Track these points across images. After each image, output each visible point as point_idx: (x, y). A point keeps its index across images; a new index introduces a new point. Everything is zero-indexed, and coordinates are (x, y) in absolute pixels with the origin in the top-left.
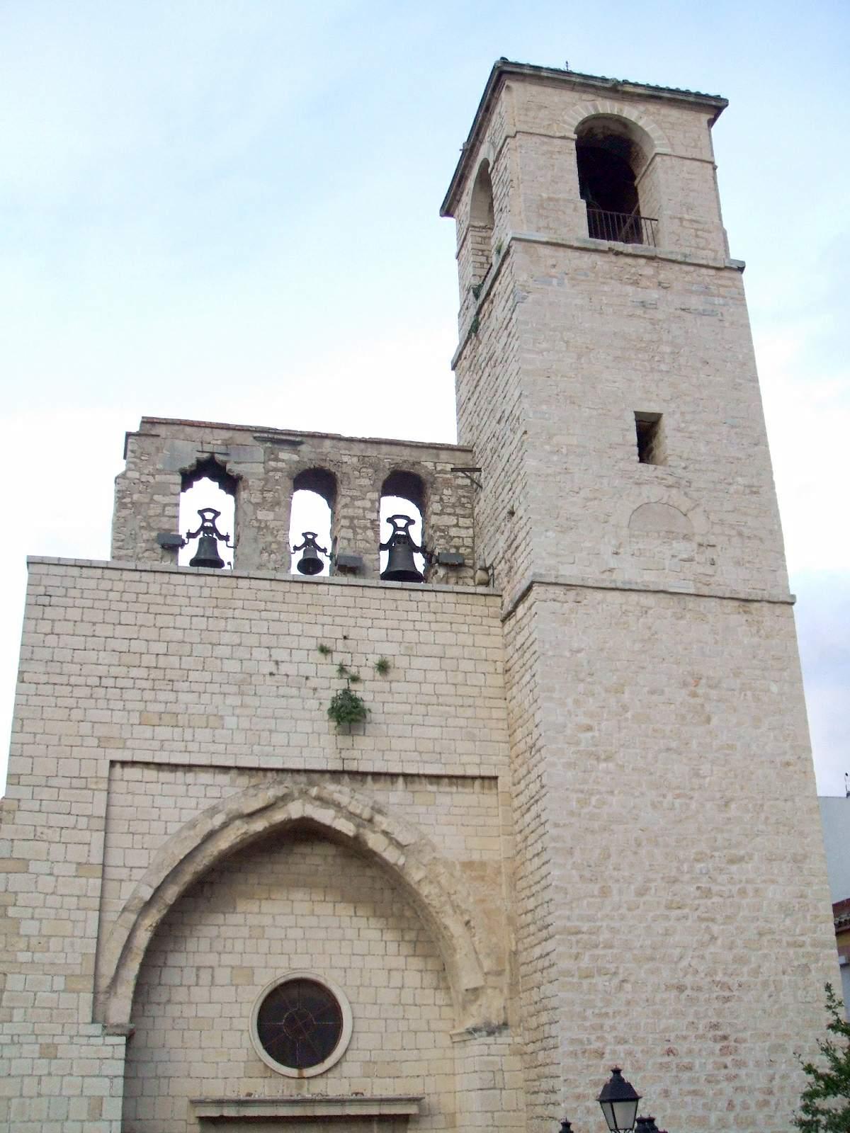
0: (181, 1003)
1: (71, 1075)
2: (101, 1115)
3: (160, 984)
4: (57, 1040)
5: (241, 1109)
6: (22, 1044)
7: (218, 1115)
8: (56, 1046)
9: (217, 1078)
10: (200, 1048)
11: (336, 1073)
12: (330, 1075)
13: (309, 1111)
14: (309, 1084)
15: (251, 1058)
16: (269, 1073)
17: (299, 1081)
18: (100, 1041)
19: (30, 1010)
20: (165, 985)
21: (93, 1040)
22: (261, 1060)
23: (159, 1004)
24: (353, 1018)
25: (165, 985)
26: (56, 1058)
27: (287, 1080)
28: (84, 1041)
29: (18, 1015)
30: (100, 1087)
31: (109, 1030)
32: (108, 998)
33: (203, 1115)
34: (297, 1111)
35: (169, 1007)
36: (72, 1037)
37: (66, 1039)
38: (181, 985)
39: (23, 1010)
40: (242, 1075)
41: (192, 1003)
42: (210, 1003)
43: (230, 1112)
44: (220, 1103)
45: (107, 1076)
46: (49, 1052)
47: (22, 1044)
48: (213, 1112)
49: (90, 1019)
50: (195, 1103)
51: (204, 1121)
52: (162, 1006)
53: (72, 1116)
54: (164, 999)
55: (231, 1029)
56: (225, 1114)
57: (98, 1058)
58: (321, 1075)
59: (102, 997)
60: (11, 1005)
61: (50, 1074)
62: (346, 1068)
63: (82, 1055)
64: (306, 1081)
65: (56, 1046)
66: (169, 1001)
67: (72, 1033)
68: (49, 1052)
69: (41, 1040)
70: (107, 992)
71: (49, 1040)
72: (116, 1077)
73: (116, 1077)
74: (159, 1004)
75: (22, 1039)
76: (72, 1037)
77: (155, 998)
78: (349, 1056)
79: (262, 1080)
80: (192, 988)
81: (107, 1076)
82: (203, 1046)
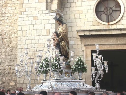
0: (74, 7)
1: (41, 24)
2: (50, 34)
3: (68, 3)
4: (37, 15)
5: (90, 33)
6: (28, 17)
7: (84, 34)
8: (37, 17)
9: (85, 26)
10: (79, 18)
11: (119, 23)
12: (118, 24)
13: (110, 33)
14: (111, 26)
15: (94, 20)
16: (99, 24)
17: (108, 26)
18: (48, 15)
19: (30, 8)
20: (69, 3)
21: (46, 15)
22: (97, 21)
23: (68, 8)
24: (124, 7)
25: (69, 3)
26: (37, 20)
27: (105, 26)
28: (44, 15)
29: (27, 9)
30: (49, 27)
31: (51, 11)
32: (51, 4)
33: (80, 35)
34: (107, 33)
35: (70, 8)
36: (41, 14)
37: (39, 15)
38: (73, 2)
39: (28, 8)
40: (92, 25)
41: (77, 7)
42: (82, 6)
43: (87, 33)
44: (84, 31)
45: (50, 24)
46: (35, 19)
47: (28, 17)
48: (82, 34)
49: (45, 9)
50: (78, 31)
51: (81, 36)
52: (69, 8)
53: (42, 35)
54: (69, 6)
55: (88, 13)
56: (86, 34)
57: (48, 19)
58: (115, 24)
59: (49, 4)
60: (25, 7)
61: (36, 24)
62: (122, 22)
63: (44, 19)
64: (110, 26)
65: (37, 17)
66: (70, 7)
67: (41, 13)
68: (35, 19)
69: (33, 15)
70: (50, 3)
71: (35, 15)
72: (53, 24)
73: (53, 24)
74: (68, 8)
75: (29, 16)
76: (41, 14)
77: (66, 6)
78: (123, 18)
79: (97, 26)
80: (76, 3)
81: (50, 24)
82: (80, 18)
